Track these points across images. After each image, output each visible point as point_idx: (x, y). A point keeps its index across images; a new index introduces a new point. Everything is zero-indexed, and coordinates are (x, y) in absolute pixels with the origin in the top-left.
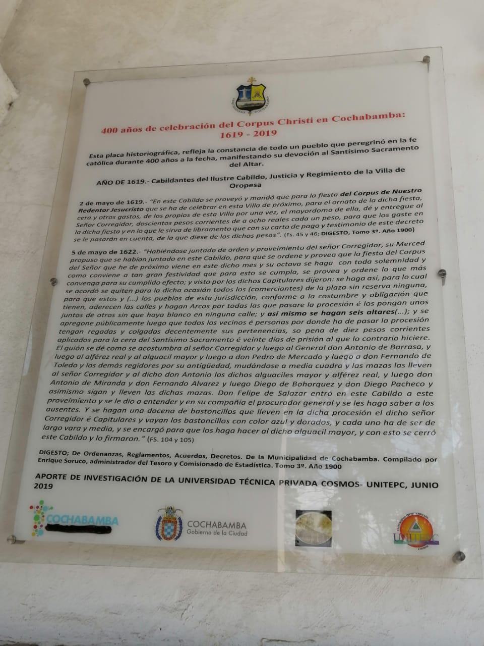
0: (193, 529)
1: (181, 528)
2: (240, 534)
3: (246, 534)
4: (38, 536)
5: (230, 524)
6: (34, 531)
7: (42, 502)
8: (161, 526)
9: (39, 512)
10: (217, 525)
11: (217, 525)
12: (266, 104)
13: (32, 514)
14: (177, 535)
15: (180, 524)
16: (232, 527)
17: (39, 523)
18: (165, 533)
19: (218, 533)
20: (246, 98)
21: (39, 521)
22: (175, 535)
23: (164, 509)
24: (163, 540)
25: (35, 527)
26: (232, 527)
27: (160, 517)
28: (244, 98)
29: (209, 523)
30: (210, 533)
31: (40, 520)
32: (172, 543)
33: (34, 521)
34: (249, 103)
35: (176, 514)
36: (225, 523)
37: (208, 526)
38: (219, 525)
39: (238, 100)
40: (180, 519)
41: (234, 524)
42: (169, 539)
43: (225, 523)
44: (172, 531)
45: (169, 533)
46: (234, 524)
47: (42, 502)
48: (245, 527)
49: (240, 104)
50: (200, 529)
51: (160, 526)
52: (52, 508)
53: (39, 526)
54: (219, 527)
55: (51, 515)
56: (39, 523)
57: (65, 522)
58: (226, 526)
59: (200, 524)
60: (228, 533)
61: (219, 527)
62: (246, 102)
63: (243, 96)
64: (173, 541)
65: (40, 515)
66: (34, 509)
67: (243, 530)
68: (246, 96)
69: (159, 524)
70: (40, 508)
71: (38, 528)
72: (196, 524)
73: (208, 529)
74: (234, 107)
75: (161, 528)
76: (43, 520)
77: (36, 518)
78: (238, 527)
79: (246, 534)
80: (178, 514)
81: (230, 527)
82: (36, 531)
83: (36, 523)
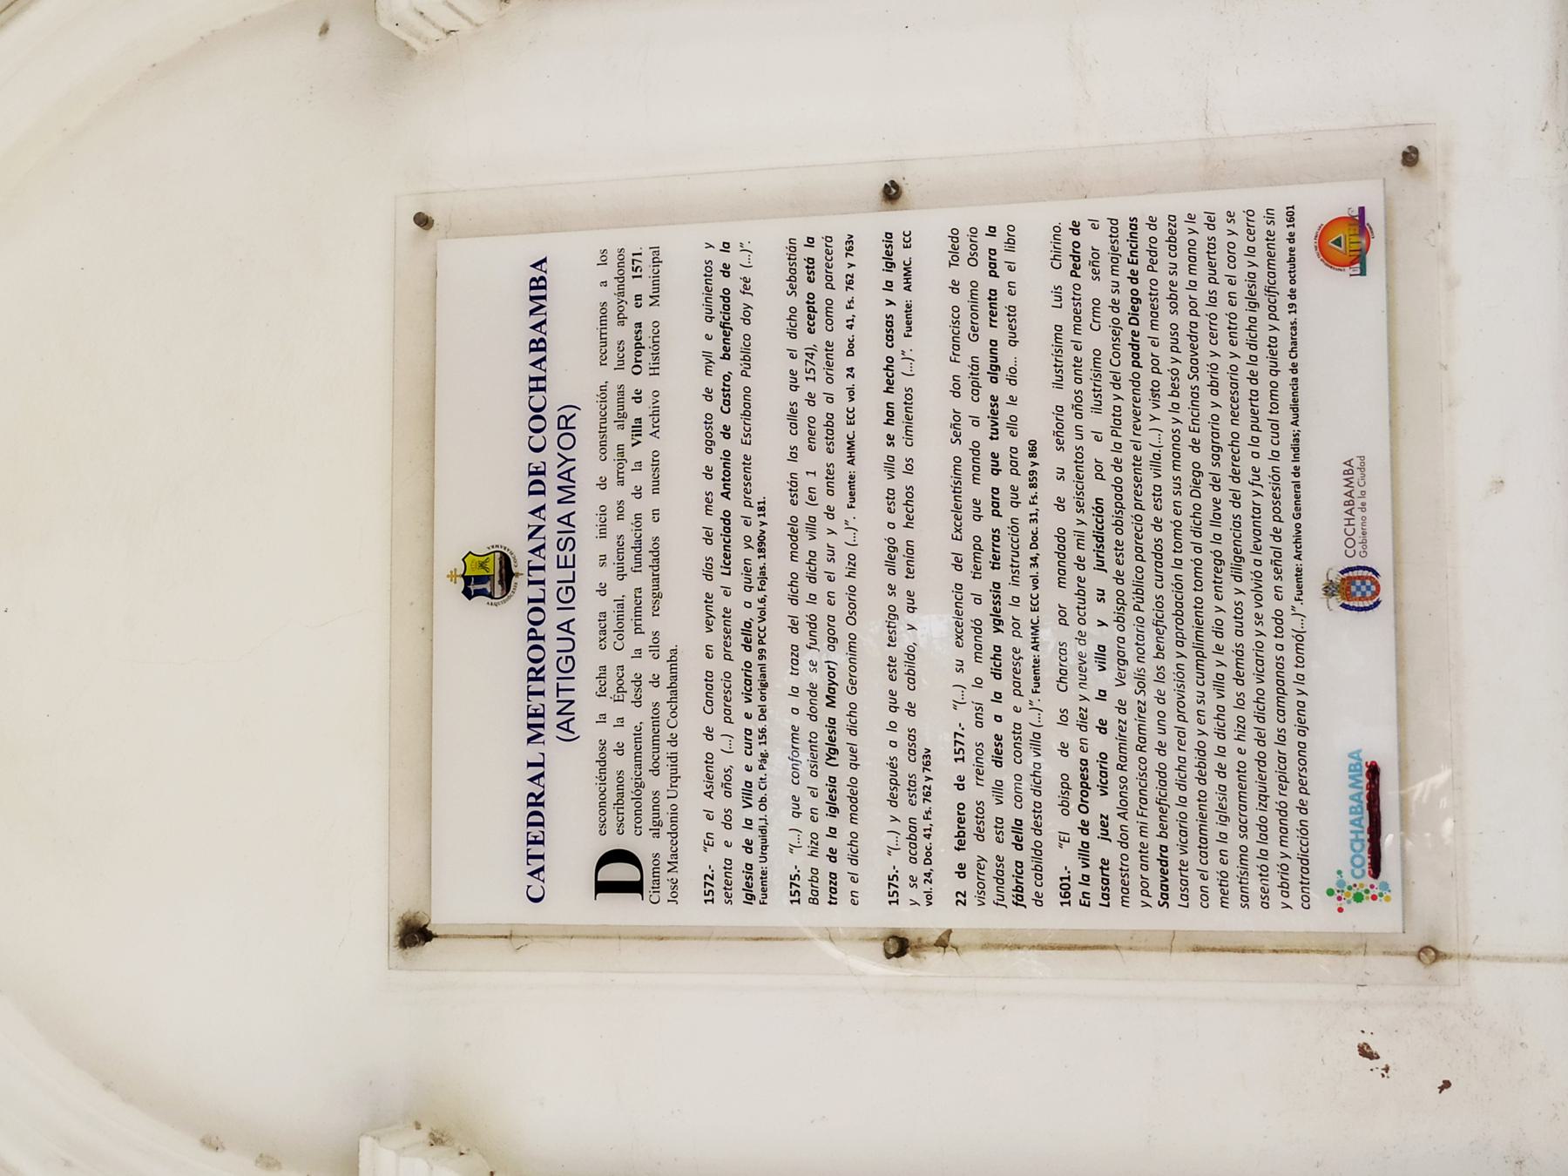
0: (1358, 548)
1: (1359, 568)
2: (1362, 468)
3: (1362, 458)
4: (1390, 891)
5: (1347, 486)
6: (1382, 898)
7: (1330, 892)
8: (1356, 604)
9: (1348, 895)
10: (1350, 507)
11: (1350, 507)
12: (502, 550)
13: (1352, 909)
14: (1370, 574)
15: (1352, 571)
16: (1351, 482)
17: (1367, 891)
18: (1369, 594)
19: (1364, 504)
20: (489, 583)
21: (1363, 893)
22: (1371, 577)
23: (1328, 601)
24: (1381, 596)
25: (1374, 898)
26: (1351, 482)
27: (1341, 606)
28: (487, 586)
29: (1347, 522)
30: (1364, 519)
31: (1362, 891)
32: (1386, 582)
33: (1365, 901)
34: (497, 578)
35: (1334, 580)
36: (1346, 494)
37: (1352, 522)
38: (1349, 505)
39: (491, 596)
40: (1342, 572)
41: (1347, 480)
42: (1378, 587)
43: (1346, 494)
44: (1363, 583)
45: (1368, 588)
46: (1347, 480)
47: (1330, 892)
48: (1349, 461)
49: (498, 588)
50: (1358, 537)
51: (1357, 606)
52: (1339, 872)
53: (1372, 892)
54: (1353, 505)
55: (1353, 871)
56: (1367, 891)
57: (1363, 846)
58: (1351, 492)
59: (1350, 537)
60: (1362, 489)
61: (1353, 505)
62: (496, 583)
63: (485, 589)
64: (1380, 580)
65: (1354, 891)
66: (1344, 904)
67: (1356, 463)
68: (485, 583)
69: (1353, 607)
70: (1340, 894)
71: (1377, 892)
72: (1350, 543)
73: (1357, 522)
74: (505, 602)
75: (1361, 602)
76: (1362, 885)
77: (1358, 898)
78: (1350, 472)
79: (1362, 458)
80: (1335, 577)
81: (1352, 485)
82: (1381, 895)
83: (1367, 898)
